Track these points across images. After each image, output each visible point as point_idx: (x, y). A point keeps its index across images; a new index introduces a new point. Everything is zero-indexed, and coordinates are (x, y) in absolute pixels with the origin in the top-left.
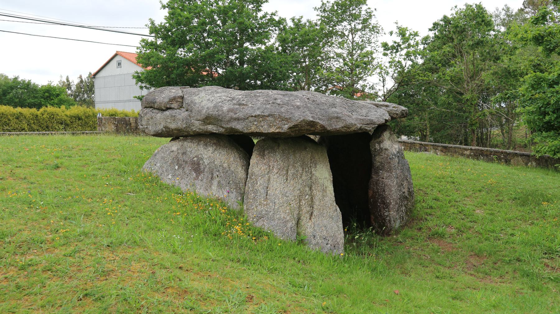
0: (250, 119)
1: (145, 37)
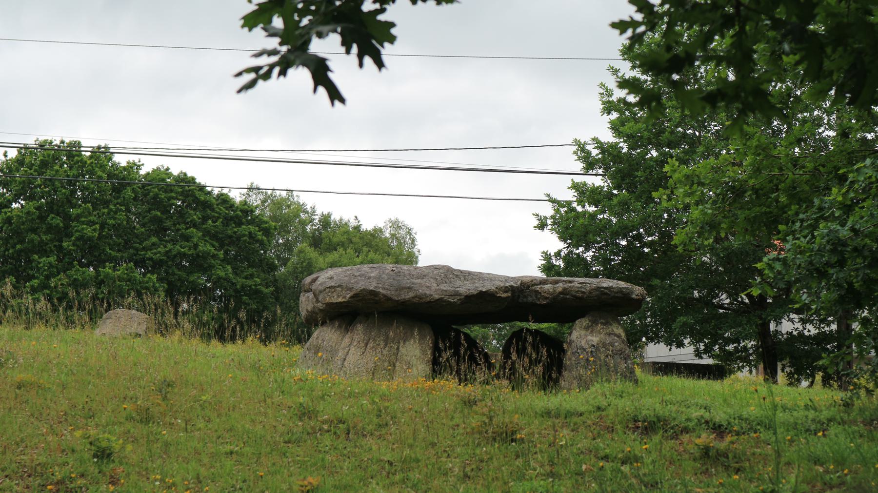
0: (327, 290)
1: (579, 179)
